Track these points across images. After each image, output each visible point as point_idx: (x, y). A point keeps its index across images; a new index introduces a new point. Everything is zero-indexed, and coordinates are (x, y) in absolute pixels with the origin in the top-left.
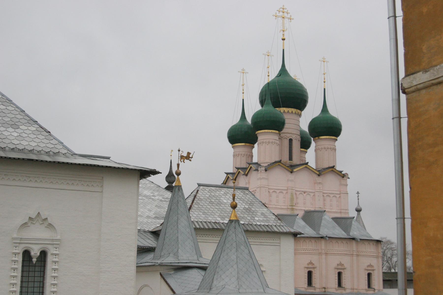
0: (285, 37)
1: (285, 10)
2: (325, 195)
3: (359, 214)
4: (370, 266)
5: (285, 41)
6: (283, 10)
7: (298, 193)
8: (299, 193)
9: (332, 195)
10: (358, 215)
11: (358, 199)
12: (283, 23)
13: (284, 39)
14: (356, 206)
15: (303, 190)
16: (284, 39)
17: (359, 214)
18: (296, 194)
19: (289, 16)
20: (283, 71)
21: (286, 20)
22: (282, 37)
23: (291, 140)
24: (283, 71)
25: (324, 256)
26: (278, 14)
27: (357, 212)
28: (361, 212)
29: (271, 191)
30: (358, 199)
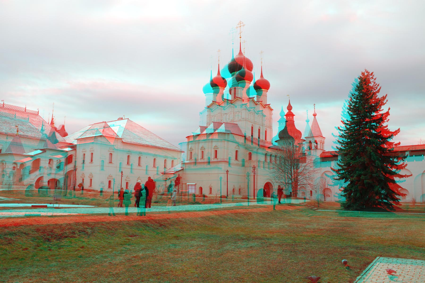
0: (241, 36)
1: (241, 22)
2: (235, 113)
3: (315, 118)
4: (216, 146)
5: (241, 38)
6: (240, 23)
7: (222, 115)
8: (223, 114)
9: (238, 112)
10: (314, 118)
11: (315, 108)
12: (240, 28)
13: (240, 37)
14: (313, 113)
15: (224, 113)
16: (240, 37)
17: (315, 118)
18: (221, 115)
19: (243, 25)
20: (240, 53)
21: (242, 27)
22: (240, 36)
23: (235, 88)
24: (240, 53)
25: (197, 144)
26: (238, 26)
27: (314, 116)
28: (316, 116)
29: (211, 117)
30: (315, 108)
